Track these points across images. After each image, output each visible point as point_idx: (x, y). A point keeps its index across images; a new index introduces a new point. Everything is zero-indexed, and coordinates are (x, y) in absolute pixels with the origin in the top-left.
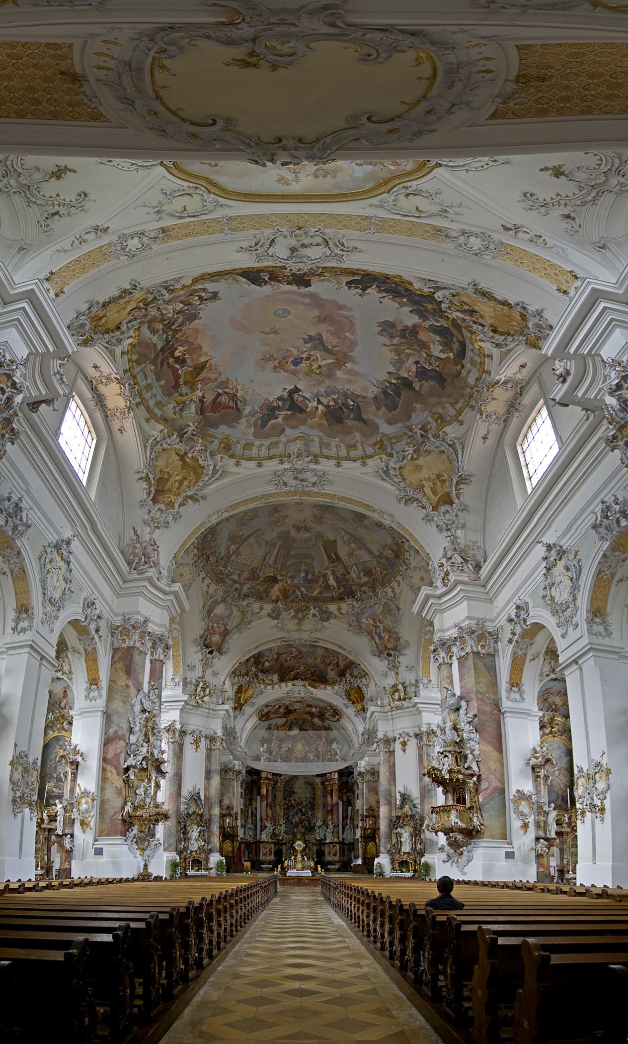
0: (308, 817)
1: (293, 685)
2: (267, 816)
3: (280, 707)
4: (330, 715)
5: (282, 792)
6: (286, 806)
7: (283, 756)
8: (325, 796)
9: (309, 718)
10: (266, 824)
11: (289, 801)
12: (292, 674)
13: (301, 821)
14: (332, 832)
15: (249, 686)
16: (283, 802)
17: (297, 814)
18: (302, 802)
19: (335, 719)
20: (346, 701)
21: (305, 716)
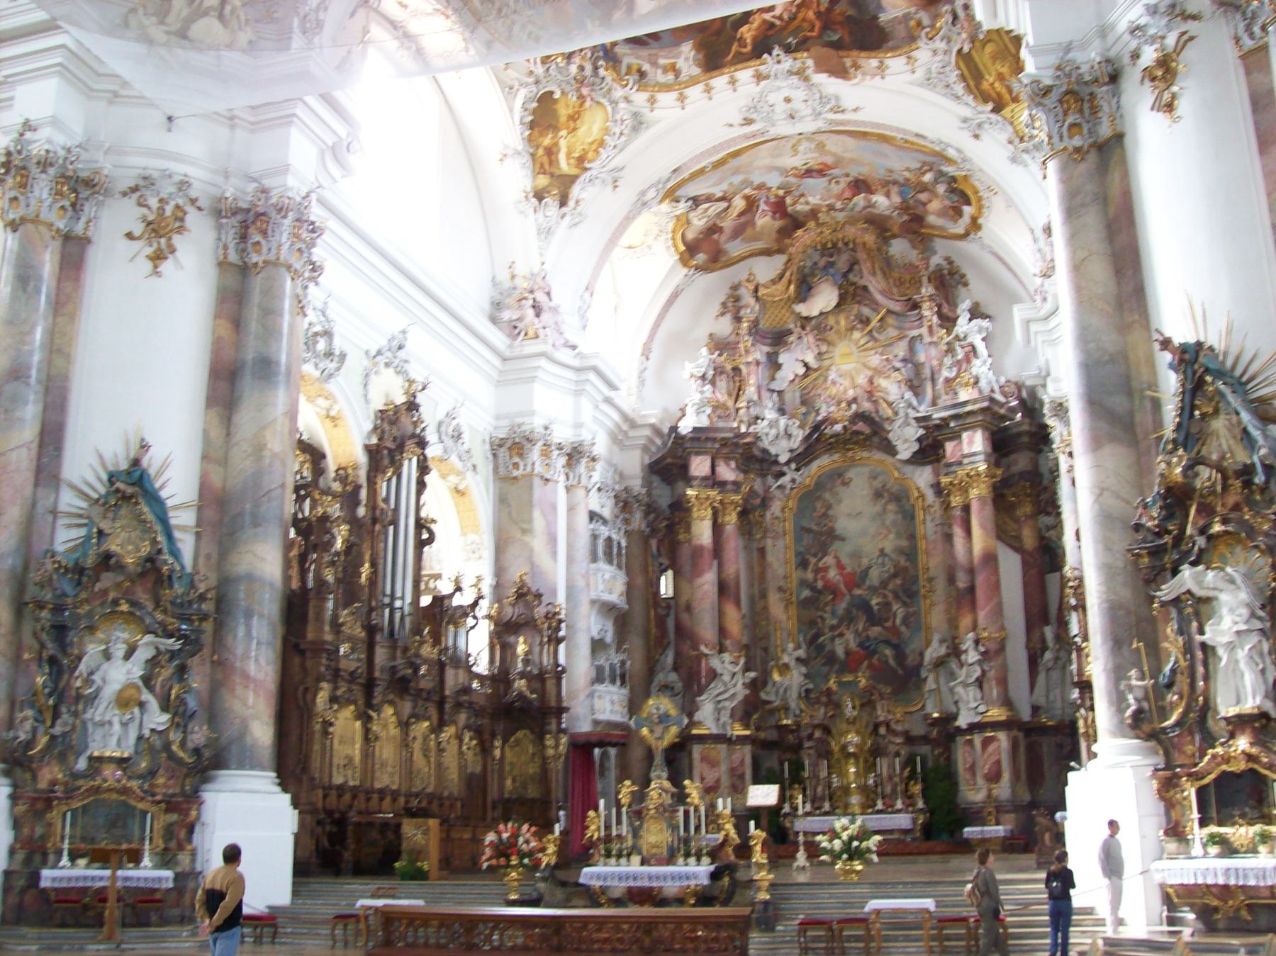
0: (895, 631)
1: (759, 77)
2: (722, 631)
3: (751, 203)
4: (942, 213)
5: (789, 539)
6: (806, 593)
7: (788, 397)
8: (949, 538)
9: (870, 238)
10: (715, 663)
11: (817, 571)
12: (747, 32)
13: (867, 648)
14: (980, 683)
15: (582, 98)
16: (796, 575)
17: (848, 619)
18: (865, 573)
19: (960, 230)
20: (968, 108)
21: (851, 232)
